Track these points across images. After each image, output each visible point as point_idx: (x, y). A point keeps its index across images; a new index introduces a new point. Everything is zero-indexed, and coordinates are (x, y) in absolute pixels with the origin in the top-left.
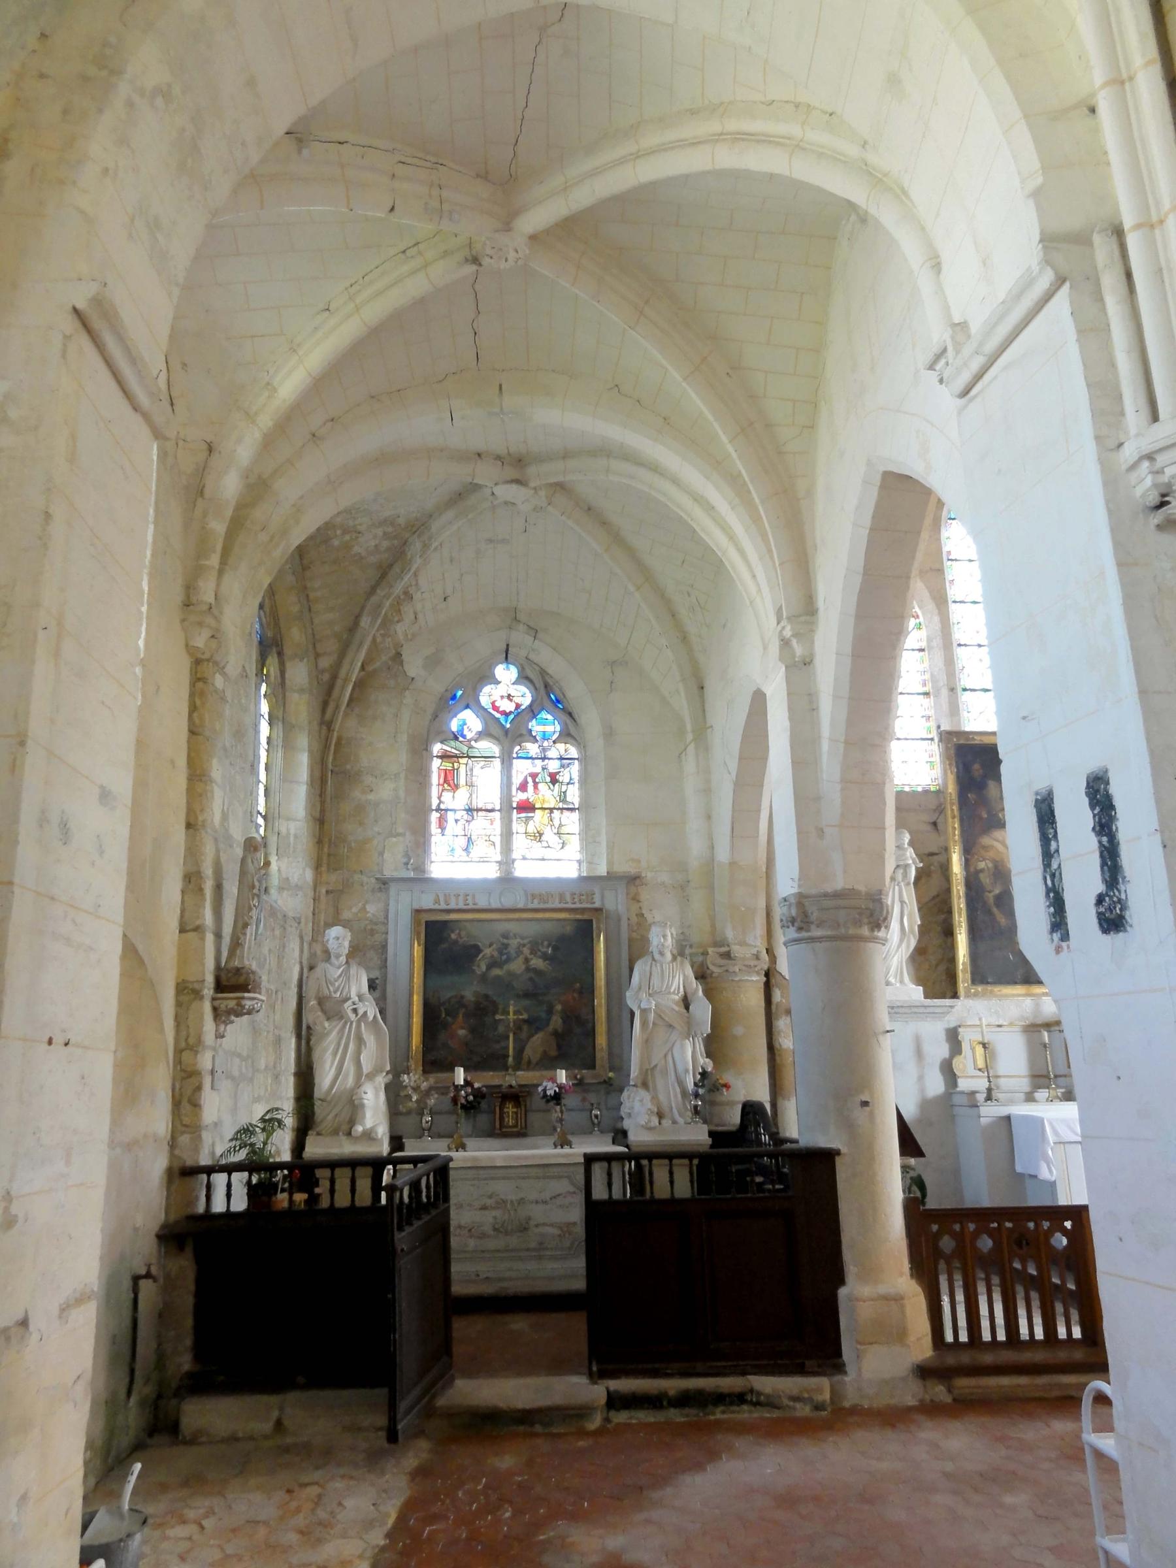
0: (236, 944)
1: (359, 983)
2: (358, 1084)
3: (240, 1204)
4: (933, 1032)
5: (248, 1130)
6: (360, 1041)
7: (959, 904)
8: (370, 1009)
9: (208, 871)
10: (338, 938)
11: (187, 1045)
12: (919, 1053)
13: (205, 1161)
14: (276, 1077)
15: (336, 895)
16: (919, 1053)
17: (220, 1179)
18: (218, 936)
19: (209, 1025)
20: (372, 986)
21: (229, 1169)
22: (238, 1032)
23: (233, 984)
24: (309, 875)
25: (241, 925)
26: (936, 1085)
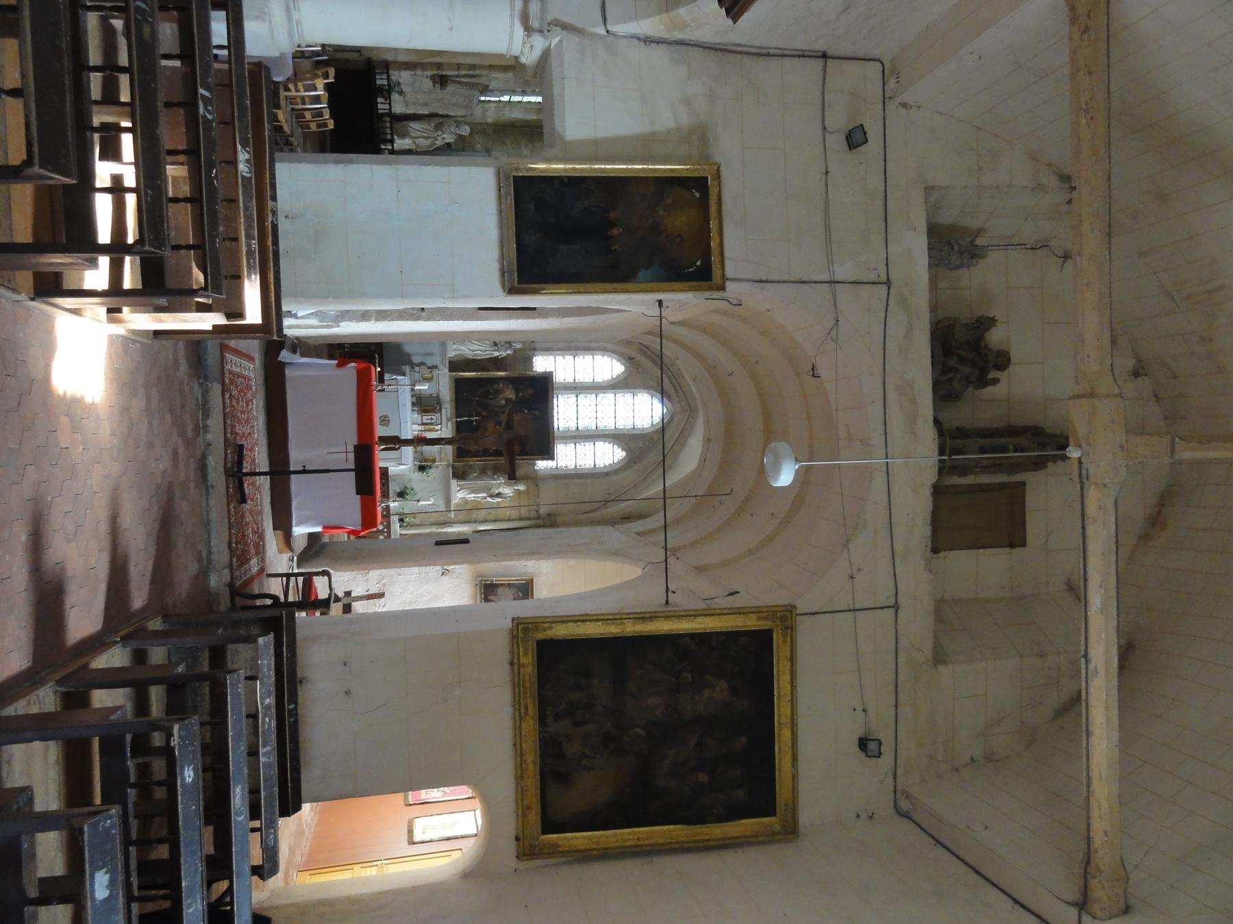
0: (454, 82)
1: (449, 139)
2: (412, 138)
3: (379, 82)
4: (436, 360)
5: (399, 84)
6: (427, 138)
7: (485, 374)
8: (439, 143)
9: (477, 72)
10: (465, 131)
11: (424, 66)
12: (428, 354)
13: (391, 72)
14: (414, 104)
15: (484, 132)
16: (428, 354)
17: (385, 76)
18: (458, 76)
19: (430, 73)
20: (448, 145)
21: (388, 78)
22: (428, 83)
23: (442, 81)
24: (490, 120)
25: (460, 83)
26: (416, 359)
